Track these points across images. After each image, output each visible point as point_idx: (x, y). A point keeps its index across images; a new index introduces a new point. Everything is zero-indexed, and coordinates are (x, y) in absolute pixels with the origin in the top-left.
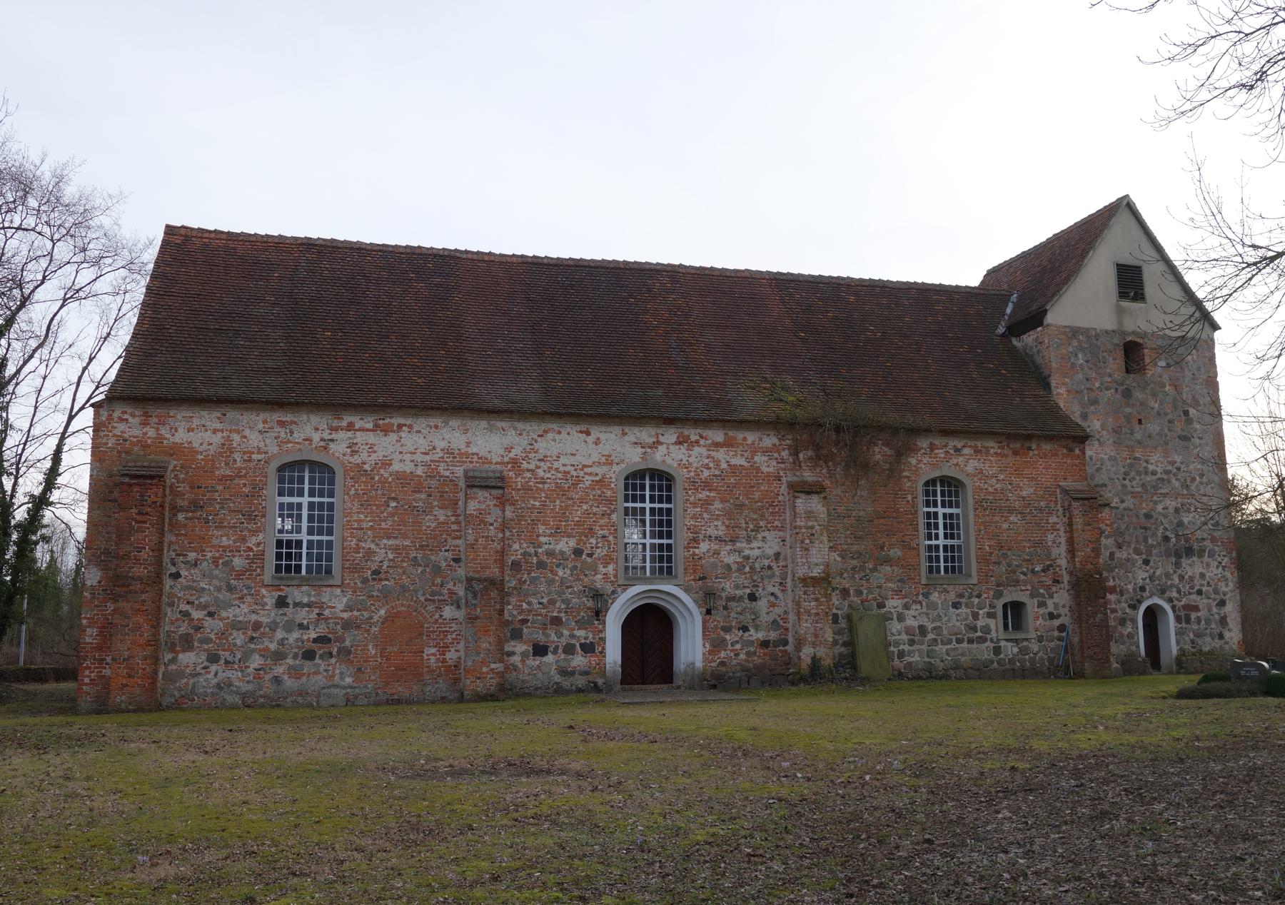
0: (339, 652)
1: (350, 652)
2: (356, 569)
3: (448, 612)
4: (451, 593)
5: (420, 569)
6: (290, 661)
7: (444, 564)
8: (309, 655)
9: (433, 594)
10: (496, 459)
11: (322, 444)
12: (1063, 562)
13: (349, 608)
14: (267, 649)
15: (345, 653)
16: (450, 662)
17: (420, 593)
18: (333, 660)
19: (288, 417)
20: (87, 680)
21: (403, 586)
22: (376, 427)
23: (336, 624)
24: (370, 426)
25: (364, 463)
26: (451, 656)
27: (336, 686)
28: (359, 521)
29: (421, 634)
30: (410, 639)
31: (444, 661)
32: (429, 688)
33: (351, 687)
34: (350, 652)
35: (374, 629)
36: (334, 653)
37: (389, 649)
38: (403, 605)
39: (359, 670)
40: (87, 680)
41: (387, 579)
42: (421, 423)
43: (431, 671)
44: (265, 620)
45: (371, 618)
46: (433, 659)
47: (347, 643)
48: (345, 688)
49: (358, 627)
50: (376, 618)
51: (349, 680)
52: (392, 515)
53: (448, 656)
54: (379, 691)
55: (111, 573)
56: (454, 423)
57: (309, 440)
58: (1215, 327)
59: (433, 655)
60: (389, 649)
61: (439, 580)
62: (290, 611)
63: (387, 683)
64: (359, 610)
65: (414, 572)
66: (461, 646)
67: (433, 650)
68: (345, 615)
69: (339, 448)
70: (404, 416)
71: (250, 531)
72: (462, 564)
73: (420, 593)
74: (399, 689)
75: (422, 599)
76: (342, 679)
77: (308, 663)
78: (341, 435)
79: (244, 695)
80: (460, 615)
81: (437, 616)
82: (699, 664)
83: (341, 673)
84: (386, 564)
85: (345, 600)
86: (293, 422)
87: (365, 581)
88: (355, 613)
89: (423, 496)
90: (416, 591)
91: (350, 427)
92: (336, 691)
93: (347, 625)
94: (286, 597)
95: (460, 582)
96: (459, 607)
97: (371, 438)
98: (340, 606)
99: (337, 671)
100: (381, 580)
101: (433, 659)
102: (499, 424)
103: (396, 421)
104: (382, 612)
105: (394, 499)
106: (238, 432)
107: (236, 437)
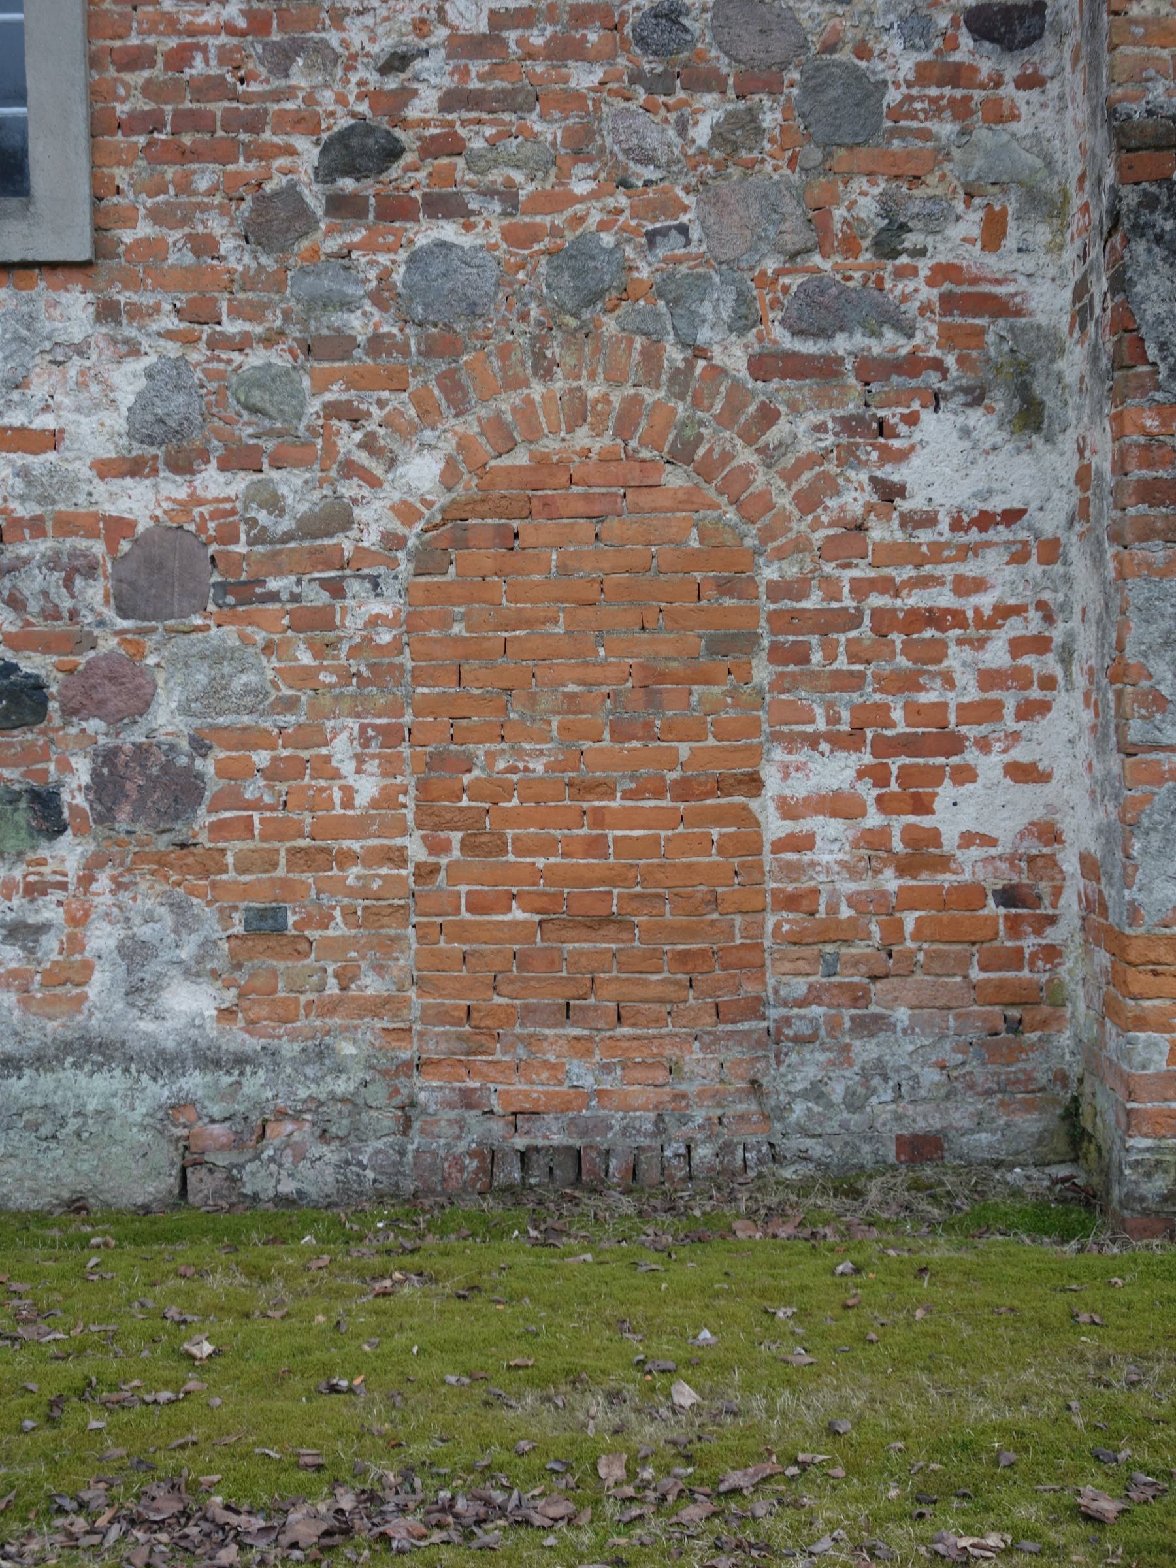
0: (107, 788)
1: (183, 791)
2: (196, 125)
3: (947, 459)
4: (970, 302)
5: (709, 115)
7: (899, 62)
9: (820, 313)
13: (158, 444)
15: (152, 793)
16: (970, 865)
17: (716, 307)
18: (68, 854)
21: (573, 258)
23: (78, 569)
26: (976, 812)
27: (96, 1051)
29: (732, 644)
30: (651, 682)
31: (923, 853)
32: (808, 1066)
33: (210, 1060)
34: (183, 791)
35: (366, 609)
36: (75, 792)
37: (489, 761)
38: (578, 412)
39: (266, 925)
41: (444, 206)
43: (820, 935)
45: (339, 518)
46: (832, 839)
47: (167, 719)
48: (164, 1063)
49: (245, 593)
50: (374, 519)
51: (190, 1004)
53: (953, 813)
54: (428, 1090)
59: (839, 805)
60: (489, 761)
61: (863, 201)
63: (478, 1032)
64: (238, 459)
65: (659, 135)
66: (1062, 735)
67: (836, 771)
68: (140, 502)
72: (1050, 55)
73: (716, 307)
74: (580, 1080)
75: (734, 357)
76: (140, 992)
80: (1035, 479)
81: (854, 497)
83: (134, 953)
84: (434, 76)
85: (128, 381)
87: (274, 222)
88: (214, 483)
90: (677, 293)
92: (98, 1087)
93: (162, 577)
95: (1046, 205)
96: (1030, 417)
98: (96, 432)
99: (102, 938)
100: (396, 209)
101: (832, 839)
104: (421, 472)
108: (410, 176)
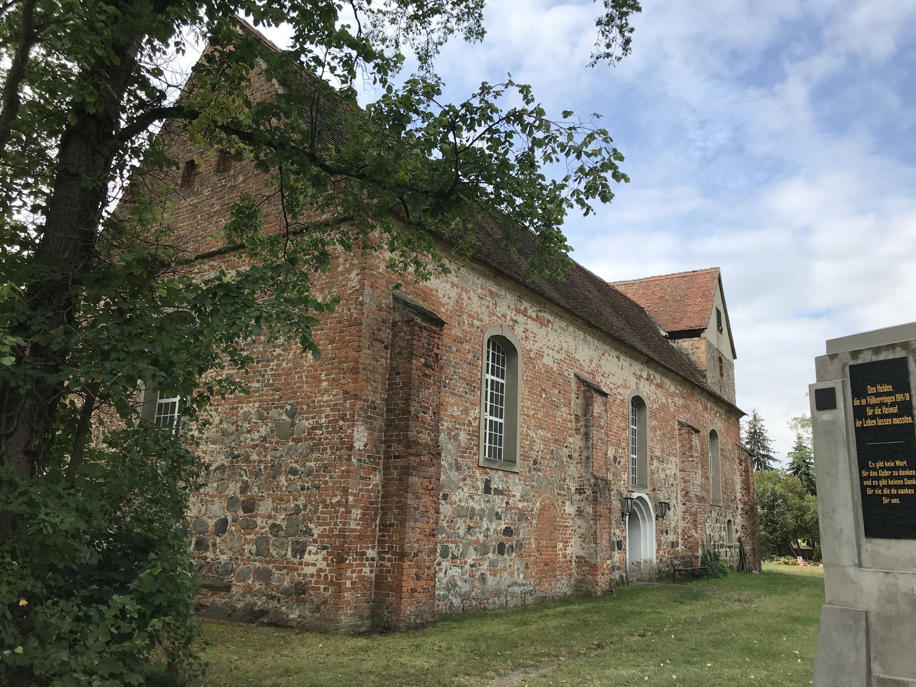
6: (490, 555)
8: (501, 549)
10: (586, 369)
11: (511, 323)
12: (739, 496)
14: (478, 541)
19: (494, 289)
20: (348, 584)
22: (537, 316)
24: (534, 315)
25: (531, 351)
26: (569, 550)
27: (515, 584)
28: (528, 408)
40: (348, 584)
42: (558, 323)
44: (477, 507)
45: (532, 510)
52: (543, 406)
55: (376, 434)
56: (571, 329)
57: (504, 316)
58: (735, 357)
62: (492, 496)
68: (520, 505)
69: (519, 330)
70: (551, 313)
71: (472, 404)
77: (501, 558)
78: (521, 318)
79: (464, 597)
82: (654, 561)
83: (518, 569)
86: (497, 295)
88: (526, 504)
89: (556, 391)
91: (525, 313)
92: (516, 588)
94: (490, 481)
97: (532, 326)
102: (588, 338)
103: (547, 316)
104: (538, 504)
105: (544, 390)
106: (467, 292)
107: (465, 296)
108: (538, 466)
